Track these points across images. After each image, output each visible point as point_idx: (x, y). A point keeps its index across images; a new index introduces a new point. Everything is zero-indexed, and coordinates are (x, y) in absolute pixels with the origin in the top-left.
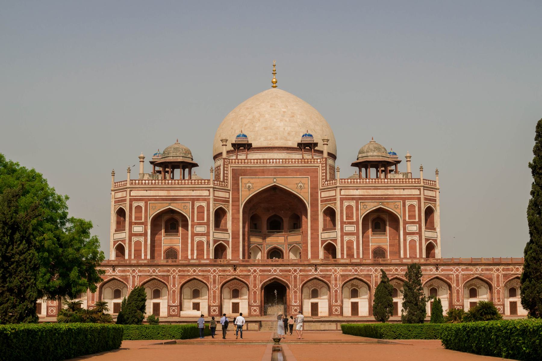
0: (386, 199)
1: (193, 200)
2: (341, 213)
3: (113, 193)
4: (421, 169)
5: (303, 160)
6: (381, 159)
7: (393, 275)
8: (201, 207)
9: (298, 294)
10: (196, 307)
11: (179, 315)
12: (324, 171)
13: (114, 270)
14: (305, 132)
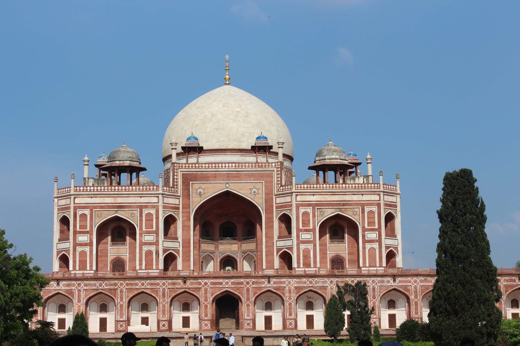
0: (344, 205)
1: (141, 208)
2: (297, 220)
3: (56, 200)
5: (257, 164)
6: (339, 162)
8: (149, 215)
9: (250, 308)
10: (145, 321)
12: (279, 176)
13: (58, 284)
14: (259, 135)
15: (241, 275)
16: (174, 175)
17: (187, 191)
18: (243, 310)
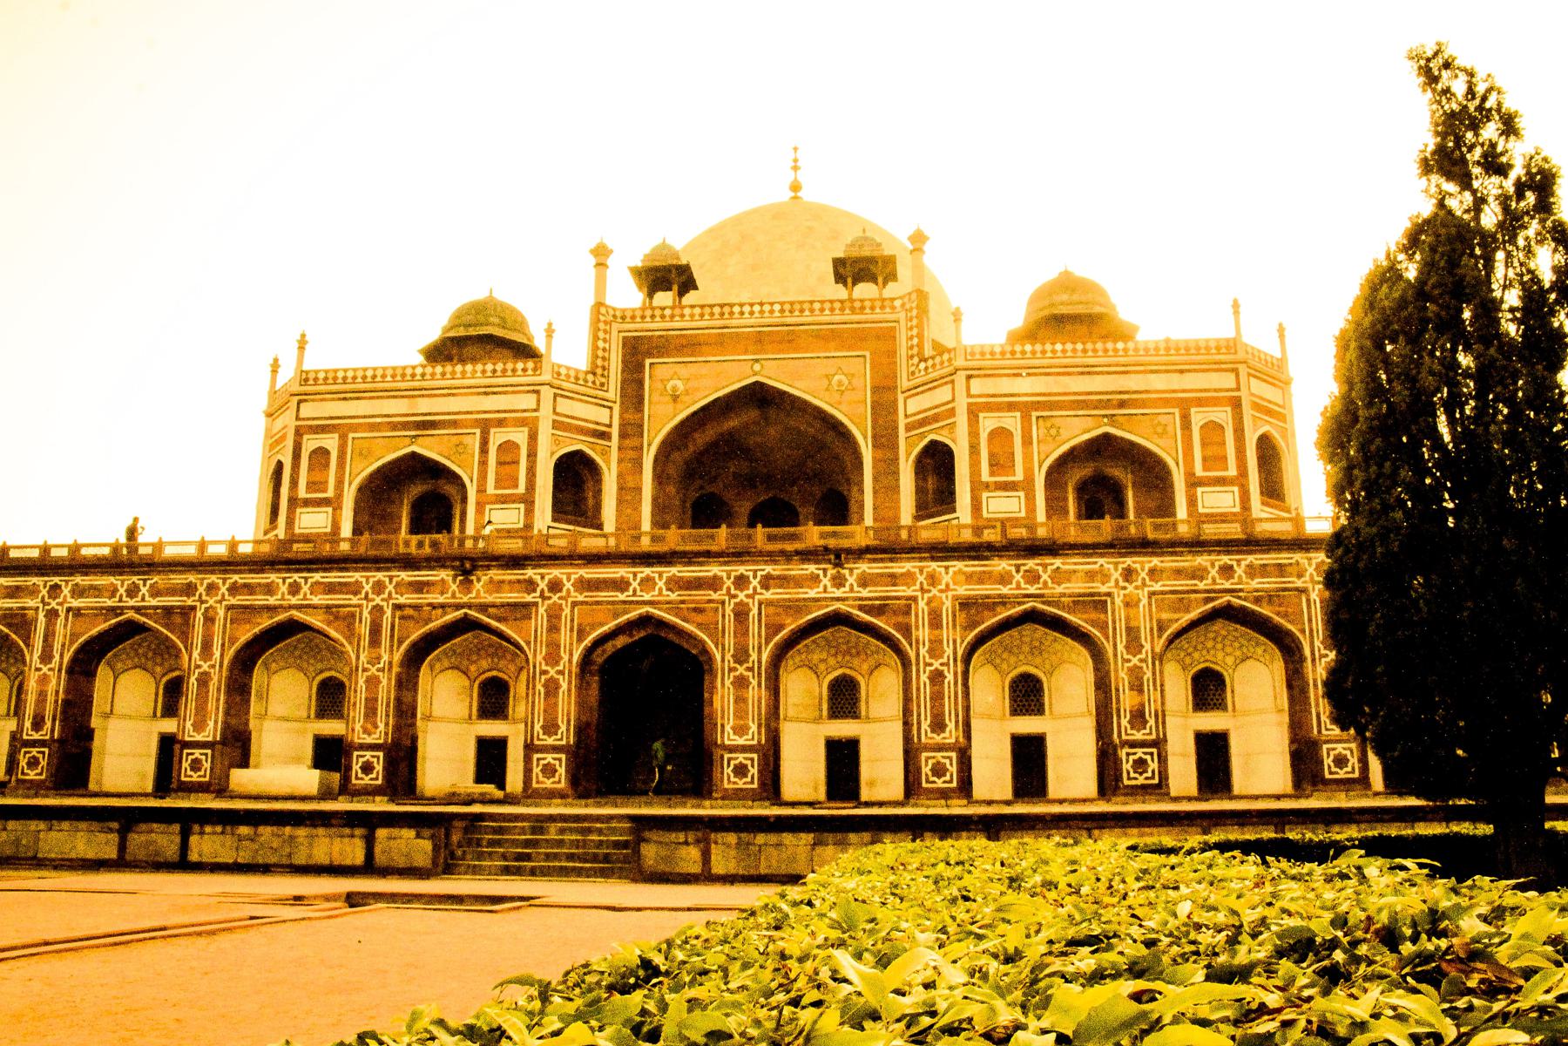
0: (1122, 404)
1: (485, 426)
2: (971, 454)
4: (1236, 305)
7: (1210, 595)
8: (508, 447)
11: (220, 788)
12: (915, 332)
15: (714, 548)
16: (596, 338)
17: (634, 385)
18: (717, 704)
